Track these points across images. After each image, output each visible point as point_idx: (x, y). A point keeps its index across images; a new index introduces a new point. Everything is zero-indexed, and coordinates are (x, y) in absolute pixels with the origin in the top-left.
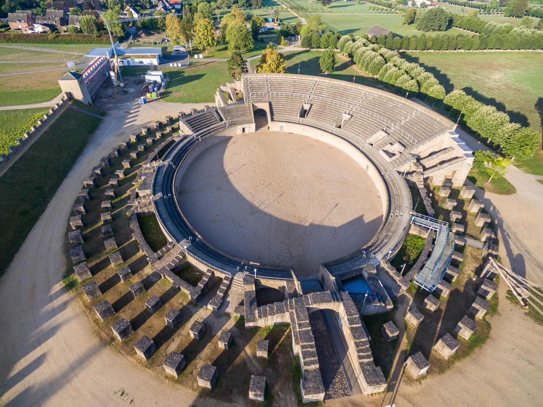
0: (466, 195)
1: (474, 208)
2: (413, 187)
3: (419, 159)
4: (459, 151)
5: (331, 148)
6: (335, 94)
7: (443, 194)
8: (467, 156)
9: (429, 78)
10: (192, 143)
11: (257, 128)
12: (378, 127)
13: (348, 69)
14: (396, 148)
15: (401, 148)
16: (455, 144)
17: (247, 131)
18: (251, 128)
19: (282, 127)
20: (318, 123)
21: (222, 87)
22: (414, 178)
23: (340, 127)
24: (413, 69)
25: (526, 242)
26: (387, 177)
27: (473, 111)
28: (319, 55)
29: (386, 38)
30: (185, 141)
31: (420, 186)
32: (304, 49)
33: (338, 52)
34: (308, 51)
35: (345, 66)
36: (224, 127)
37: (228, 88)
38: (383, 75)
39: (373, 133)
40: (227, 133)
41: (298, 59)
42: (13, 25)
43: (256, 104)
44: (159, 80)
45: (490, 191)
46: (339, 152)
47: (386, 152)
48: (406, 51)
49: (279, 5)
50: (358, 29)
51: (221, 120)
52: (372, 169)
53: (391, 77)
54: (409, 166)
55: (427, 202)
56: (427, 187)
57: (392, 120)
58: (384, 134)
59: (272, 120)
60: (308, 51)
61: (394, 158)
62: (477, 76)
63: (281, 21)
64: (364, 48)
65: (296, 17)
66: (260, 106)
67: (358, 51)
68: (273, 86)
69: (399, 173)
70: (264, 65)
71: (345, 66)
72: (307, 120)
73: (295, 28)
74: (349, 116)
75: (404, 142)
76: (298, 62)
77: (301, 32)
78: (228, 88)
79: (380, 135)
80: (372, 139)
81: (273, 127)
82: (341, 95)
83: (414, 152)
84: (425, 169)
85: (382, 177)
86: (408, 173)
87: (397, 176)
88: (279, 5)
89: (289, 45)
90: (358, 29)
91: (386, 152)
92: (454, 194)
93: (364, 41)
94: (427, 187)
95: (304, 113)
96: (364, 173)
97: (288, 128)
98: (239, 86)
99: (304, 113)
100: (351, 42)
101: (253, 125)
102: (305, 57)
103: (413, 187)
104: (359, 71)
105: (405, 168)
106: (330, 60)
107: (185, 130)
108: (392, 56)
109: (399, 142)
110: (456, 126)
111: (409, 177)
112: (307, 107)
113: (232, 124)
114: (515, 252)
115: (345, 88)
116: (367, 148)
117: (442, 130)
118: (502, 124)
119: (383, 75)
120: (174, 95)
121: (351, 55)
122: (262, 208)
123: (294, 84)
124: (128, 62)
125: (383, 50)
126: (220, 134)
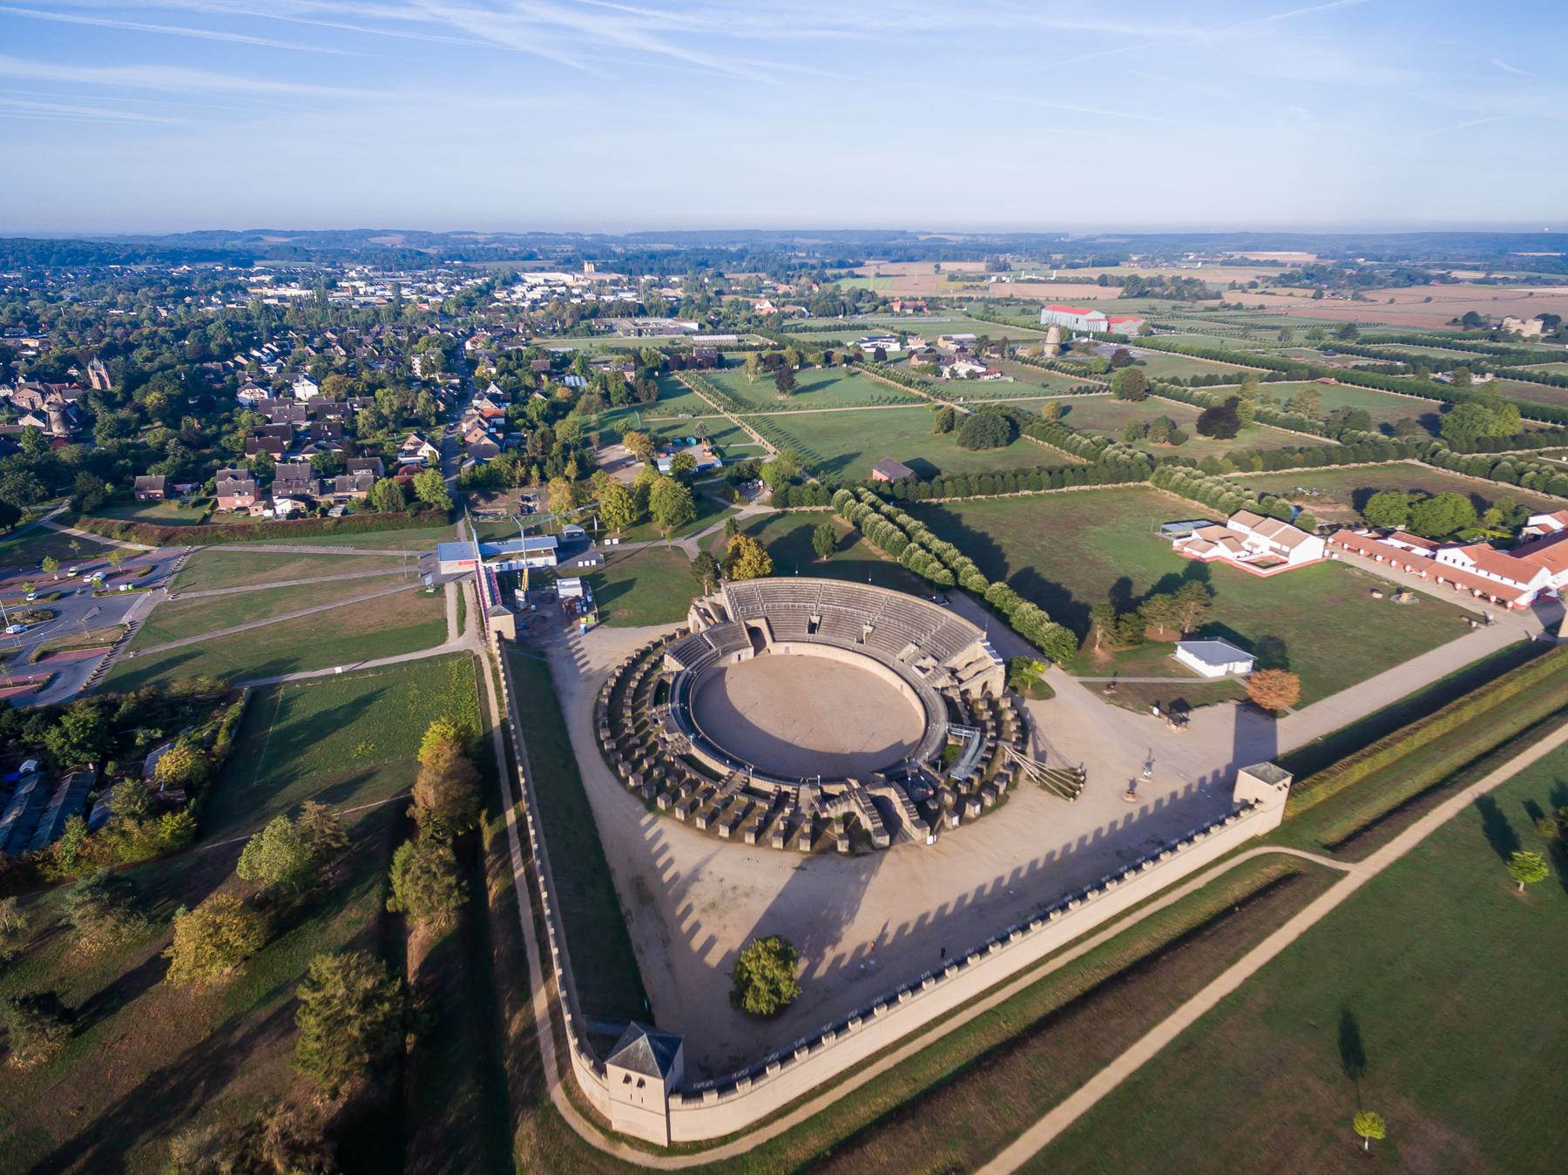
0: (1005, 704)
1: (1009, 716)
2: (949, 703)
3: (953, 672)
4: (991, 661)
5: (855, 668)
6: (848, 600)
7: (981, 706)
8: (997, 663)
9: (966, 564)
10: (688, 680)
11: (756, 653)
12: (907, 639)
13: (857, 545)
14: (929, 662)
15: (934, 662)
16: (986, 653)
17: (743, 658)
18: (749, 653)
19: (787, 648)
20: (834, 640)
21: (697, 603)
22: (951, 693)
23: (862, 642)
24: (945, 551)
25: (1052, 740)
26: (923, 695)
27: (1014, 609)
28: (803, 522)
29: (906, 484)
30: (681, 679)
31: (958, 700)
32: (779, 510)
33: (833, 512)
34: (784, 514)
35: (850, 540)
36: (716, 657)
37: (706, 604)
38: (907, 560)
39: (902, 646)
40: (722, 664)
41: (773, 532)
42: (563, 593)
43: (748, 622)
44: (579, 592)
45: (1029, 698)
46: (866, 673)
47: (920, 668)
48: (942, 501)
49: (689, 391)
50: (856, 455)
51: (711, 648)
52: (906, 687)
53: (917, 562)
54: (944, 681)
55: (965, 715)
56: (966, 701)
57: (922, 631)
58: (915, 647)
59: (774, 641)
60: (784, 514)
61: (928, 673)
62: (1044, 543)
63: (712, 439)
64: (876, 516)
65: (738, 428)
66: (753, 623)
67: (866, 520)
68: (769, 595)
69: (935, 689)
70: (741, 563)
71: (850, 540)
72: (818, 635)
73: (751, 468)
74: (871, 629)
75: (937, 654)
76: (774, 537)
77: (763, 475)
78: (706, 604)
79: (911, 648)
80: (903, 654)
81: (775, 649)
82: (857, 601)
83: (947, 665)
84: (961, 681)
85: (918, 695)
86: (943, 689)
87: (933, 691)
88: (689, 391)
89: (750, 501)
90: (856, 455)
91: (920, 668)
92: (993, 704)
93: (873, 497)
94: (966, 701)
95: (813, 628)
96: (898, 694)
97: (796, 649)
98: (722, 598)
99: (813, 628)
100: (853, 501)
101: (752, 649)
102: (783, 529)
103: (949, 703)
104: (873, 548)
105: (940, 684)
106: (830, 541)
107: (671, 665)
108: (917, 529)
109: (933, 656)
110: (985, 634)
111: (946, 692)
112: (815, 620)
113: (726, 652)
114: (1041, 749)
115: (860, 592)
116: (898, 665)
117: (973, 640)
118: (1042, 623)
119: (907, 560)
120: (616, 615)
121: (857, 524)
122: (797, 742)
123: (793, 590)
124: (510, 565)
125: (903, 518)
126: (716, 666)
